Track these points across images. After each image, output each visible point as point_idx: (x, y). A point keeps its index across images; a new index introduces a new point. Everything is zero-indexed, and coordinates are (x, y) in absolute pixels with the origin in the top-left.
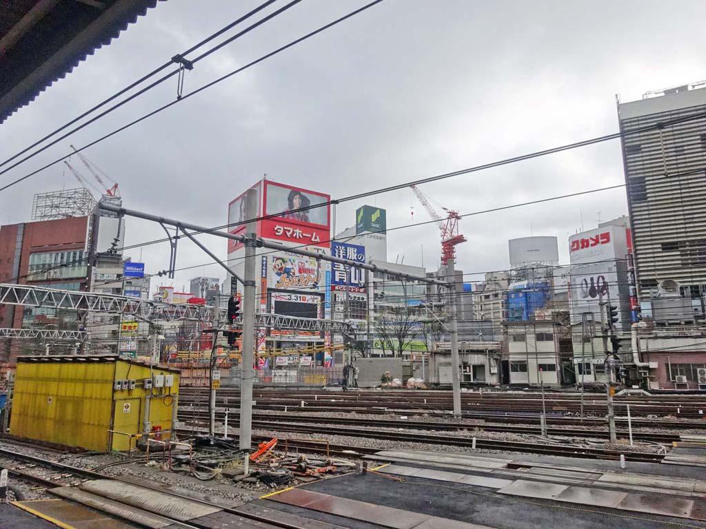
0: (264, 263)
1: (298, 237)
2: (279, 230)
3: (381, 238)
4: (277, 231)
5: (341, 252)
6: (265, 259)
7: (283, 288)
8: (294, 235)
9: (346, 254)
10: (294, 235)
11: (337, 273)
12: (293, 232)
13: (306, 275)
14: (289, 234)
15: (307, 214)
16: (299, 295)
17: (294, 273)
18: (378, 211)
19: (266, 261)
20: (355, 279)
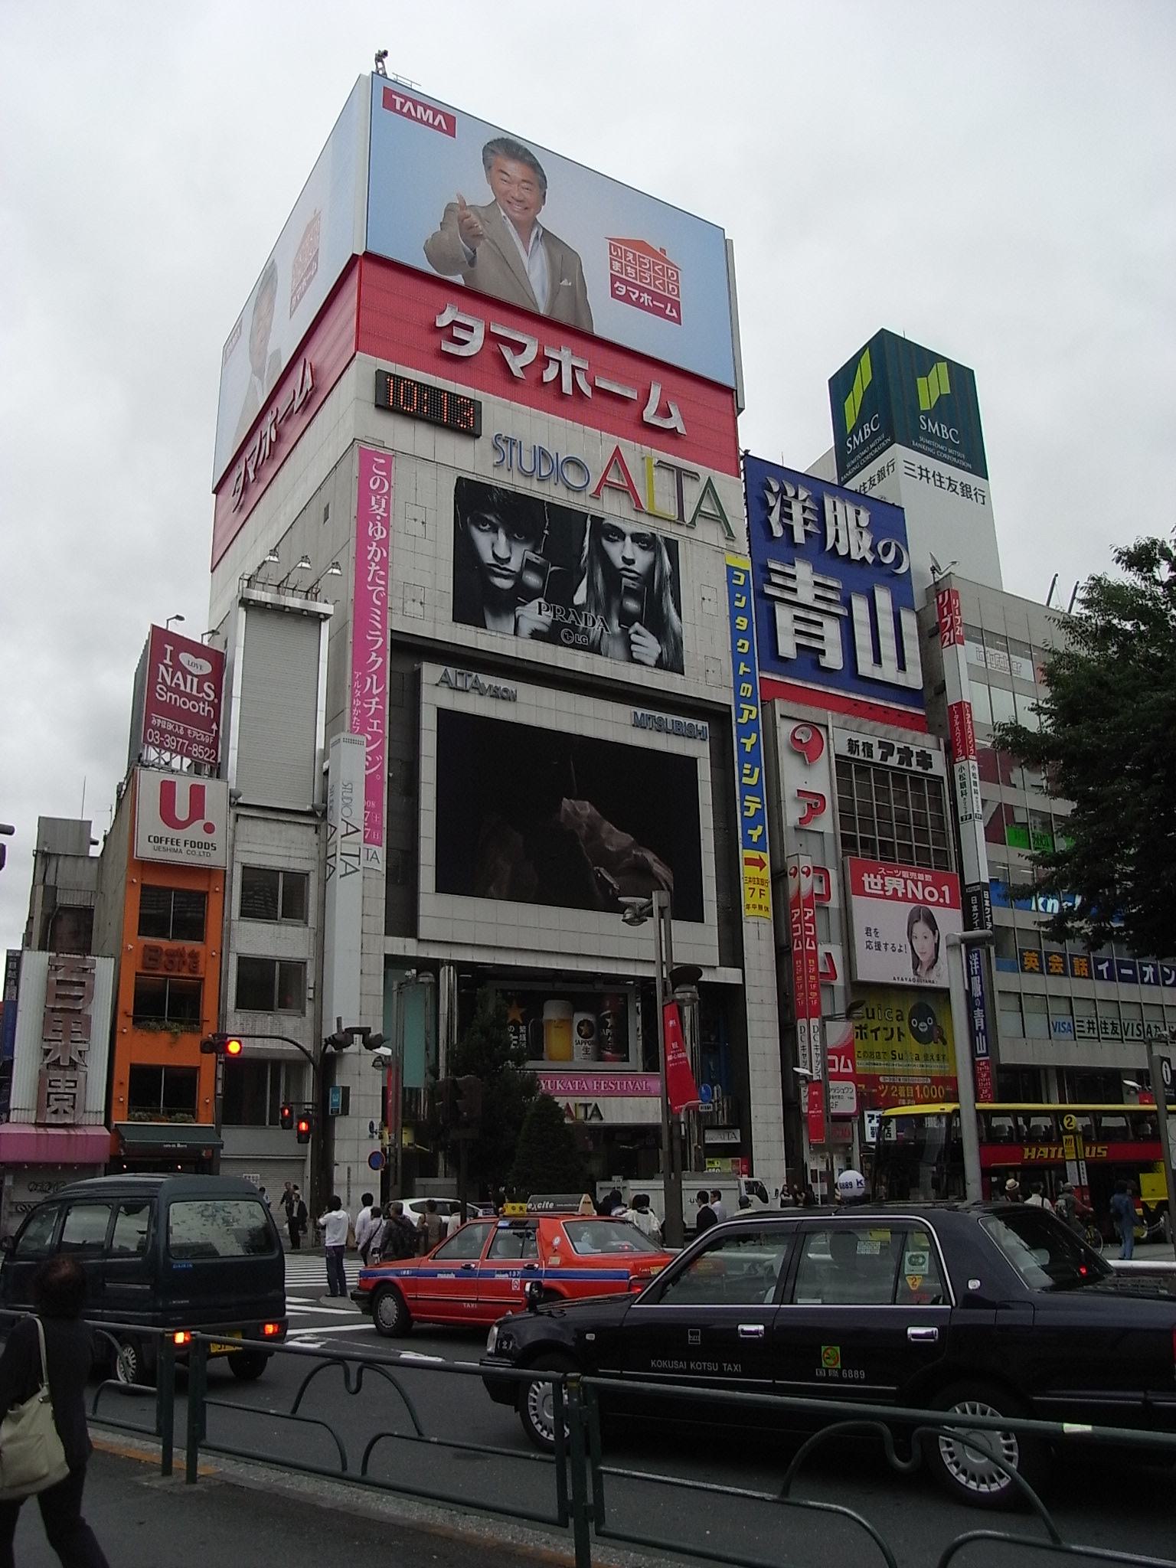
1: (567, 387)
2: (458, 333)
3: (966, 491)
4: (447, 332)
5: (796, 510)
8: (549, 375)
9: (822, 523)
10: (549, 375)
11: (784, 617)
12: (543, 360)
14: (516, 363)
18: (942, 367)
20: (878, 660)
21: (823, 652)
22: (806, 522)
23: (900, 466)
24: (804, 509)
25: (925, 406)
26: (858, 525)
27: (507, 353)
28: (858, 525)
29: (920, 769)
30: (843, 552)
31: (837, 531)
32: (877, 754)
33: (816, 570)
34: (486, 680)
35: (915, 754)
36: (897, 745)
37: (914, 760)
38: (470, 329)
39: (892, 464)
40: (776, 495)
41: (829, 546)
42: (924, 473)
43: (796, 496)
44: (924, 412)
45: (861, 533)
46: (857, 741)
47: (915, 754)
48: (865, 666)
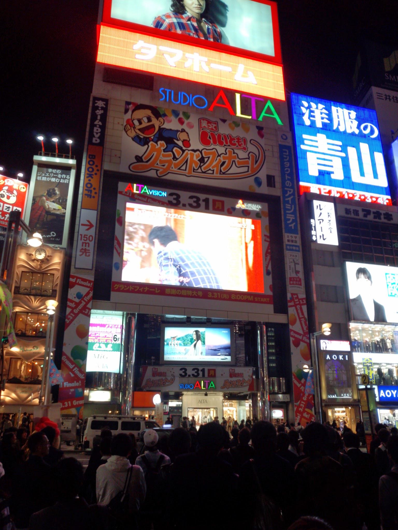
0: (99, 112)
2: (143, 51)
6: (100, 104)
7: (152, 174)
9: (330, 119)
13: (221, 150)
15: (219, 29)
16: (202, 196)
17: (187, 143)
19: (105, 109)
21: (333, 173)
22: (322, 118)
23: (375, 96)
24: (321, 113)
25: (387, 69)
26: (350, 118)
27: (166, 56)
28: (350, 118)
29: (386, 221)
30: (342, 129)
31: (339, 121)
32: (361, 214)
33: (328, 137)
35: (382, 214)
36: (372, 210)
37: (382, 217)
38: (150, 49)
39: (371, 95)
40: (307, 108)
41: (335, 128)
42: (388, 97)
43: (317, 108)
44: (388, 72)
45: (352, 122)
46: (350, 209)
47: (382, 214)
48: (356, 177)
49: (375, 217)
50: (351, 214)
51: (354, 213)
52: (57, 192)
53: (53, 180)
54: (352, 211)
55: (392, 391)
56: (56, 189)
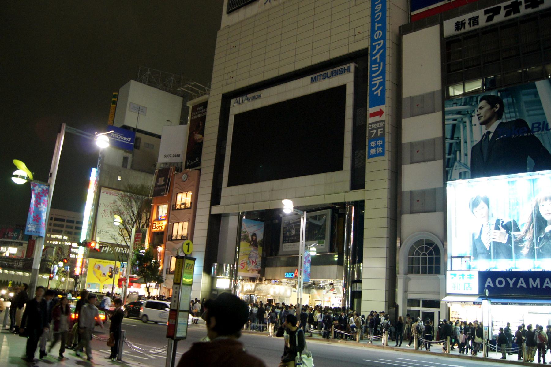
29: (530, 10)
34: (250, 96)
46: (465, 20)
49: (507, 14)
50: (464, 28)
51: (470, 24)
52: (201, 125)
53: (199, 116)
54: (467, 22)
55: (508, 279)
56: (200, 122)
